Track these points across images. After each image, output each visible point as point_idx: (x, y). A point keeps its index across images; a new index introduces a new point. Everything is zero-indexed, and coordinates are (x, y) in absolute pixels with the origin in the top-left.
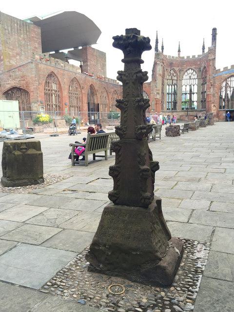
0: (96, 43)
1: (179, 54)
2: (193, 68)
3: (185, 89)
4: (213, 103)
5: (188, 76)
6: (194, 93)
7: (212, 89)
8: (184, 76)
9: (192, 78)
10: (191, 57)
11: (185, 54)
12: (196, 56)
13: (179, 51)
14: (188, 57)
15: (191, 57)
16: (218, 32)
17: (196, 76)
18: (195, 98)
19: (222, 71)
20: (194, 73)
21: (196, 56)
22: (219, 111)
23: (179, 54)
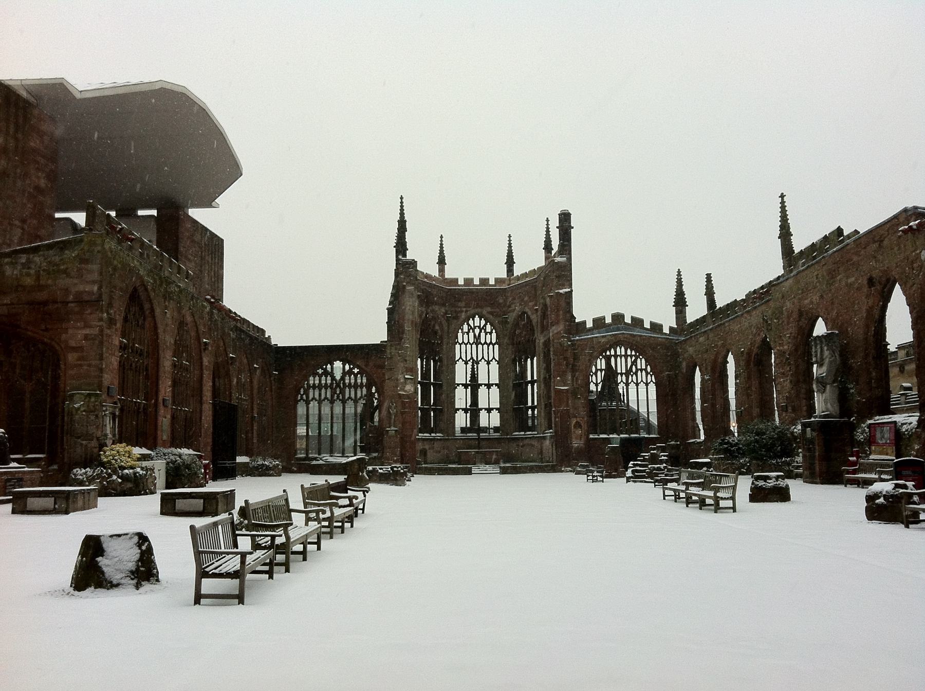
0: (210, 206)
1: (442, 271)
2: (485, 312)
3: (461, 374)
5: (471, 334)
6: (489, 386)
8: (460, 335)
9: (483, 341)
10: (476, 282)
11: (457, 271)
12: (492, 282)
14: (468, 281)
15: (476, 282)
17: (494, 335)
18: (490, 398)
19: (590, 330)
21: (492, 282)
23: (442, 271)
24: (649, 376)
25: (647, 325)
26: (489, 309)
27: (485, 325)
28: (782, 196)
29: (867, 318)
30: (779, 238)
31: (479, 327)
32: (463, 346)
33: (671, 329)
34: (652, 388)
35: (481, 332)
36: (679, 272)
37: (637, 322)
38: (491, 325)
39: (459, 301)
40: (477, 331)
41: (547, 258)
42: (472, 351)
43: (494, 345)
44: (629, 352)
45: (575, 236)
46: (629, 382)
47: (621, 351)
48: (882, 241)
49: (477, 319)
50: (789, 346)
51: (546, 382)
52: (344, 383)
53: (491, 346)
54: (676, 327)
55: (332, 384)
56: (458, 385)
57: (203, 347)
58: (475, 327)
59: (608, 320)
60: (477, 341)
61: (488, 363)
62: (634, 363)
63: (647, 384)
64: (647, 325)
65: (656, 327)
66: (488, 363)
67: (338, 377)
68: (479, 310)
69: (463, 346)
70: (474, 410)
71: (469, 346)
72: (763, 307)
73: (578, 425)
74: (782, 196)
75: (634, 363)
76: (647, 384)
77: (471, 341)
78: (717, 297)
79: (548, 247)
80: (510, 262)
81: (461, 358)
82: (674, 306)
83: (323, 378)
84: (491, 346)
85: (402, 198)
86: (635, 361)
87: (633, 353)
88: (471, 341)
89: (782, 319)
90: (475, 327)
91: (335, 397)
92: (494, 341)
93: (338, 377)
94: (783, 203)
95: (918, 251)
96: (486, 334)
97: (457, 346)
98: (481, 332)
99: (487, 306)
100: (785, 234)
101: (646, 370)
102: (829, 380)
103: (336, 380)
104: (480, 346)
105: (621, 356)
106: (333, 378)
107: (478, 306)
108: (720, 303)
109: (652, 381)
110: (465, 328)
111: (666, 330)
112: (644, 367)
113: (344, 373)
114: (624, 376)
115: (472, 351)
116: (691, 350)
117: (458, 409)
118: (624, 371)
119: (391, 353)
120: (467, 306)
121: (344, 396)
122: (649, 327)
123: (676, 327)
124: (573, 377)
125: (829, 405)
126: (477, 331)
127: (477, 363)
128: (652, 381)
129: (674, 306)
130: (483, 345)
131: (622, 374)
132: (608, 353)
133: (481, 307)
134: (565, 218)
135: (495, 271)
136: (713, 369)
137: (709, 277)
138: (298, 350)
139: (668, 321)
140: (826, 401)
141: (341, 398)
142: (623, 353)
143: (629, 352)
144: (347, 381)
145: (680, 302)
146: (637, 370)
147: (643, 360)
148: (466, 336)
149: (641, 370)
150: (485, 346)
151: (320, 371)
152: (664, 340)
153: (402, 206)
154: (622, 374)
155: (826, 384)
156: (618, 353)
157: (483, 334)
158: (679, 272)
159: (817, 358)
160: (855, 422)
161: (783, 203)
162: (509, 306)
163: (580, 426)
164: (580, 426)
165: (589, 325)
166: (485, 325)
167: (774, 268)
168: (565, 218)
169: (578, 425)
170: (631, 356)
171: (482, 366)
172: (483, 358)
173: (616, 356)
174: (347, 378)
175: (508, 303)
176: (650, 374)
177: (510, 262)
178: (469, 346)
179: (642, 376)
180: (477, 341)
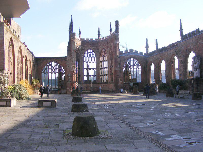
1: (80, 36)
2: (92, 48)
3: (85, 66)
4: (120, 77)
5: (88, 54)
7: (118, 66)
8: (85, 54)
9: (91, 56)
10: (90, 40)
12: (94, 40)
13: (80, 33)
14: (88, 39)
15: (90, 40)
16: (119, 23)
17: (95, 55)
20: (93, 53)
22: (125, 84)
23: (80, 36)
25: (139, 53)
26: (93, 47)
27: (92, 52)
31: (90, 52)
32: (86, 58)
33: (145, 53)
34: (140, 69)
35: (91, 54)
36: (147, 38)
37: (136, 52)
38: (94, 52)
39: (85, 45)
40: (90, 53)
41: (111, 33)
42: (88, 59)
43: (94, 57)
44: (134, 60)
45: (120, 27)
46: (134, 68)
47: (132, 59)
49: (90, 50)
51: (110, 67)
52: (55, 68)
53: (94, 58)
55: (52, 68)
56: (85, 69)
57: (23, 57)
58: (89, 52)
59: (129, 51)
60: (90, 56)
61: (93, 62)
62: (136, 63)
63: (139, 69)
64: (139, 53)
65: (141, 53)
66: (93, 62)
67: (53, 66)
68: (91, 48)
69: (86, 58)
70: (88, 75)
71: (88, 58)
72: (175, 49)
73: (121, 80)
74: (180, 20)
75: (136, 63)
76: (139, 69)
77: (88, 56)
79: (111, 30)
80: (99, 34)
81: (85, 61)
83: (49, 66)
84: (94, 58)
85: (72, 16)
86: (136, 62)
87: (135, 60)
88: (88, 56)
90: (89, 52)
91: (53, 72)
92: (95, 56)
93: (53, 66)
94: (181, 22)
96: (92, 54)
97: (84, 58)
98: (91, 54)
99: (93, 47)
100: (181, 30)
101: (138, 65)
102: (198, 68)
103: (53, 67)
104: (91, 58)
105: (132, 61)
106: (52, 66)
107: (91, 46)
108: (160, 47)
110: (87, 52)
111: (144, 54)
112: (138, 64)
113: (55, 65)
114: (133, 67)
115: (88, 59)
116: (151, 60)
117: (85, 75)
118: (133, 65)
119: (68, 59)
120: (87, 46)
121: (55, 72)
124: (120, 66)
125: (198, 74)
126: (90, 53)
127: (90, 62)
130: (91, 57)
131: (132, 66)
132: (129, 60)
133: (91, 47)
134: (117, 22)
135: (95, 37)
137: (156, 40)
138: (42, 59)
139: (144, 52)
141: (54, 72)
142: (133, 60)
143: (134, 60)
144: (56, 68)
145: (147, 47)
146: (136, 65)
147: (138, 62)
148: (87, 55)
149: (137, 65)
150: (92, 58)
151: (48, 64)
153: (72, 18)
154: (132, 66)
156: (131, 60)
157: (91, 54)
161: (181, 22)
162: (99, 47)
163: (121, 80)
164: (121, 80)
165: (124, 52)
166: (92, 52)
167: (178, 38)
168: (117, 22)
169: (121, 80)
170: (135, 61)
171: (91, 63)
172: (92, 61)
173: (131, 61)
174: (56, 66)
175: (99, 46)
177: (99, 34)
178: (88, 58)
179: (137, 66)
180: (90, 56)
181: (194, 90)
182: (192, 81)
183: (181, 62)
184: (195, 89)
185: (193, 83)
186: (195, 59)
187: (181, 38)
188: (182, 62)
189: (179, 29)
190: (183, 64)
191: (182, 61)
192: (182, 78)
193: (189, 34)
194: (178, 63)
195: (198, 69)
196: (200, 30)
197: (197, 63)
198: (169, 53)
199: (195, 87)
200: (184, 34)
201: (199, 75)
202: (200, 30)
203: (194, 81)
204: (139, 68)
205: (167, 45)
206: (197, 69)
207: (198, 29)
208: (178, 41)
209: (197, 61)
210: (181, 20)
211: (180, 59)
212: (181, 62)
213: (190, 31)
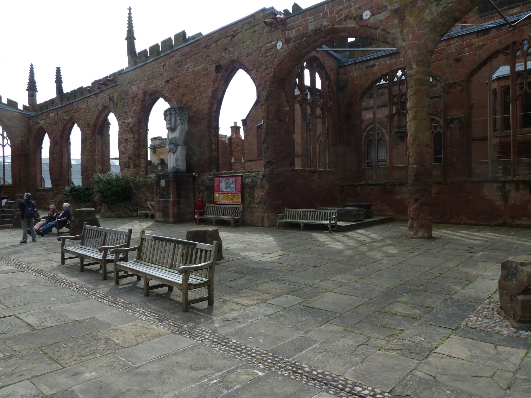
24: (5, 140)
28: (130, 9)
29: (212, 97)
30: (126, 39)
33: (24, 106)
48: (233, 36)
50: (133, 119)
54: (28, 105)
65: (12, 104)
72: (111, 90)
74: (130, 9)
78: (63, 85)
82: (27, 90)
89: (127, 99)
94: (130, 14)
95: (273, 43)
100: (131, 38)
102: (181, 143)
108: (67, 88)
109: (7, 144)
111: (20, 107)
116: (42, 123)
122: (6, 103)
123: (28, 106)
125: (179, 162)
128: (7, 144)
129: (27, 90)
136: (61, 137)
137: (58, 70)
139: (23, 101)
140: (177, 160)
145: (32, 88)
152: (18, 113)
155: (178, 145)
158: (32, 66)
159: (171, 125)
160: (196, 175)
161: (130, 14)
176: (6, 139)
181: (168, 208)
182: (163, 183)
183: (127, 127)
184: (170, 206)
185: (167, 189)
186: (173, 116)
187: (129, 63)
188: (131, 129)
189: (124, 34)
190: (133, 133)
191: (129, 124)
192: (129, 173)
193: (154, 49)
194: (118, 130)
195: (179, 148)
196: (189, 35)
197: (179, 127)
198: (93, 103)
199: (171, 200)
200: (139, 47)
201: (182, 166)
202: (189, 35)
203: (167, 182)
204: (5, 143)
205: (87, 83)
206: (176, 145)
207: (183, 34)
208: (121, 73)
209: (179, 122)
210: (131, 10)
211: (125, 118)
212: (127, 127)
213: (158, 40)
